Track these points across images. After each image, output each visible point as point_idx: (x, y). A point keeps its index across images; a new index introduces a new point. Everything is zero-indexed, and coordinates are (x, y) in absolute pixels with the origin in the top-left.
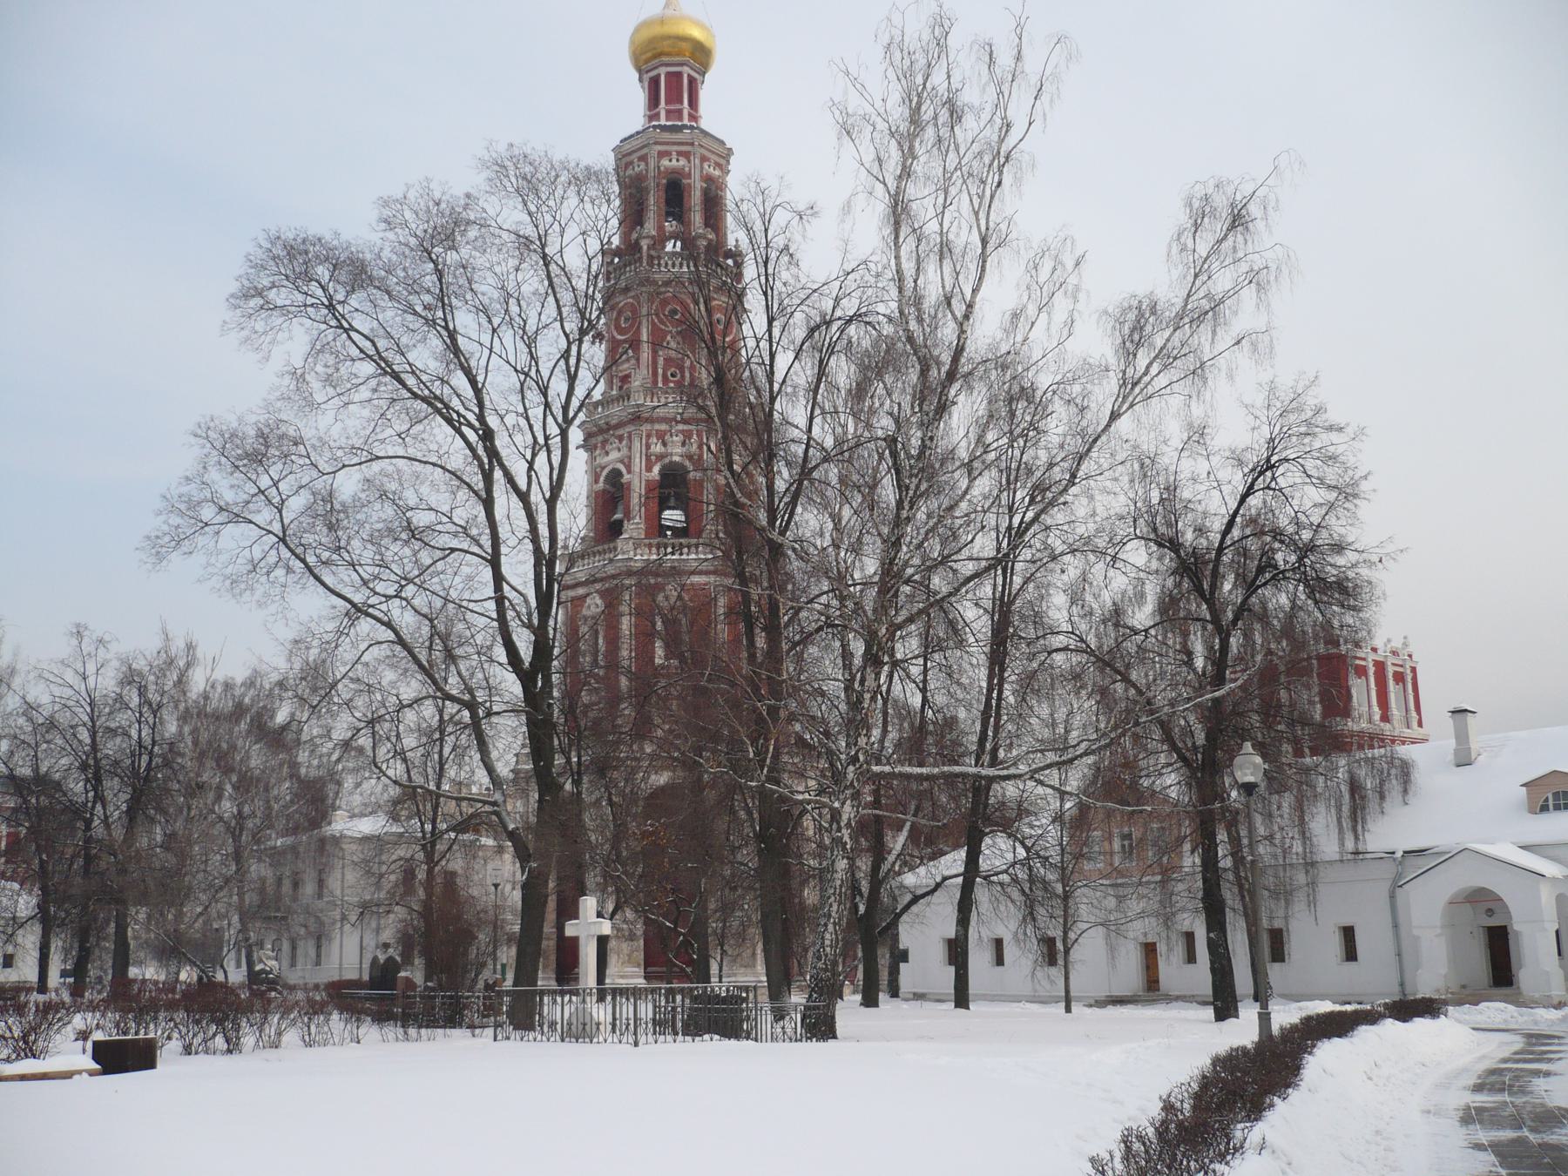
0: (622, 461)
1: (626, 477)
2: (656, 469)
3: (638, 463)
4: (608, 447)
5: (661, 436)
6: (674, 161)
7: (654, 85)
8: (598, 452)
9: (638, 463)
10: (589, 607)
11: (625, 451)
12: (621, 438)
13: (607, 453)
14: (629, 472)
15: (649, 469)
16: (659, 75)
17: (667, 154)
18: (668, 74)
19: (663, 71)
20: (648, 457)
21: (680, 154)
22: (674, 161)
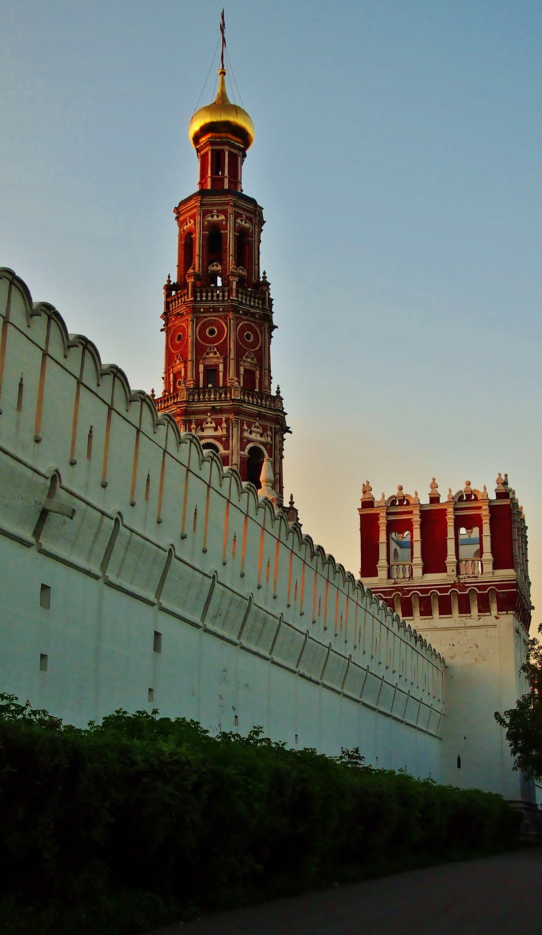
2: (246, 451)
3: (234, 442)
4: (204, 426)
5: (249, 425)
7: (218, 156)
8: (193, 426)
9: (234, 442)
11: (225, 432)
12: (219, 423)
13: (203, 430)
14: (226, 448)
15: (242, 449)
16: (223, 151)
17: (240, 215)
18: (229, 152)
19: (226, 148)
20: (242, 438)
21: (247, 218)
22: (243, 223)
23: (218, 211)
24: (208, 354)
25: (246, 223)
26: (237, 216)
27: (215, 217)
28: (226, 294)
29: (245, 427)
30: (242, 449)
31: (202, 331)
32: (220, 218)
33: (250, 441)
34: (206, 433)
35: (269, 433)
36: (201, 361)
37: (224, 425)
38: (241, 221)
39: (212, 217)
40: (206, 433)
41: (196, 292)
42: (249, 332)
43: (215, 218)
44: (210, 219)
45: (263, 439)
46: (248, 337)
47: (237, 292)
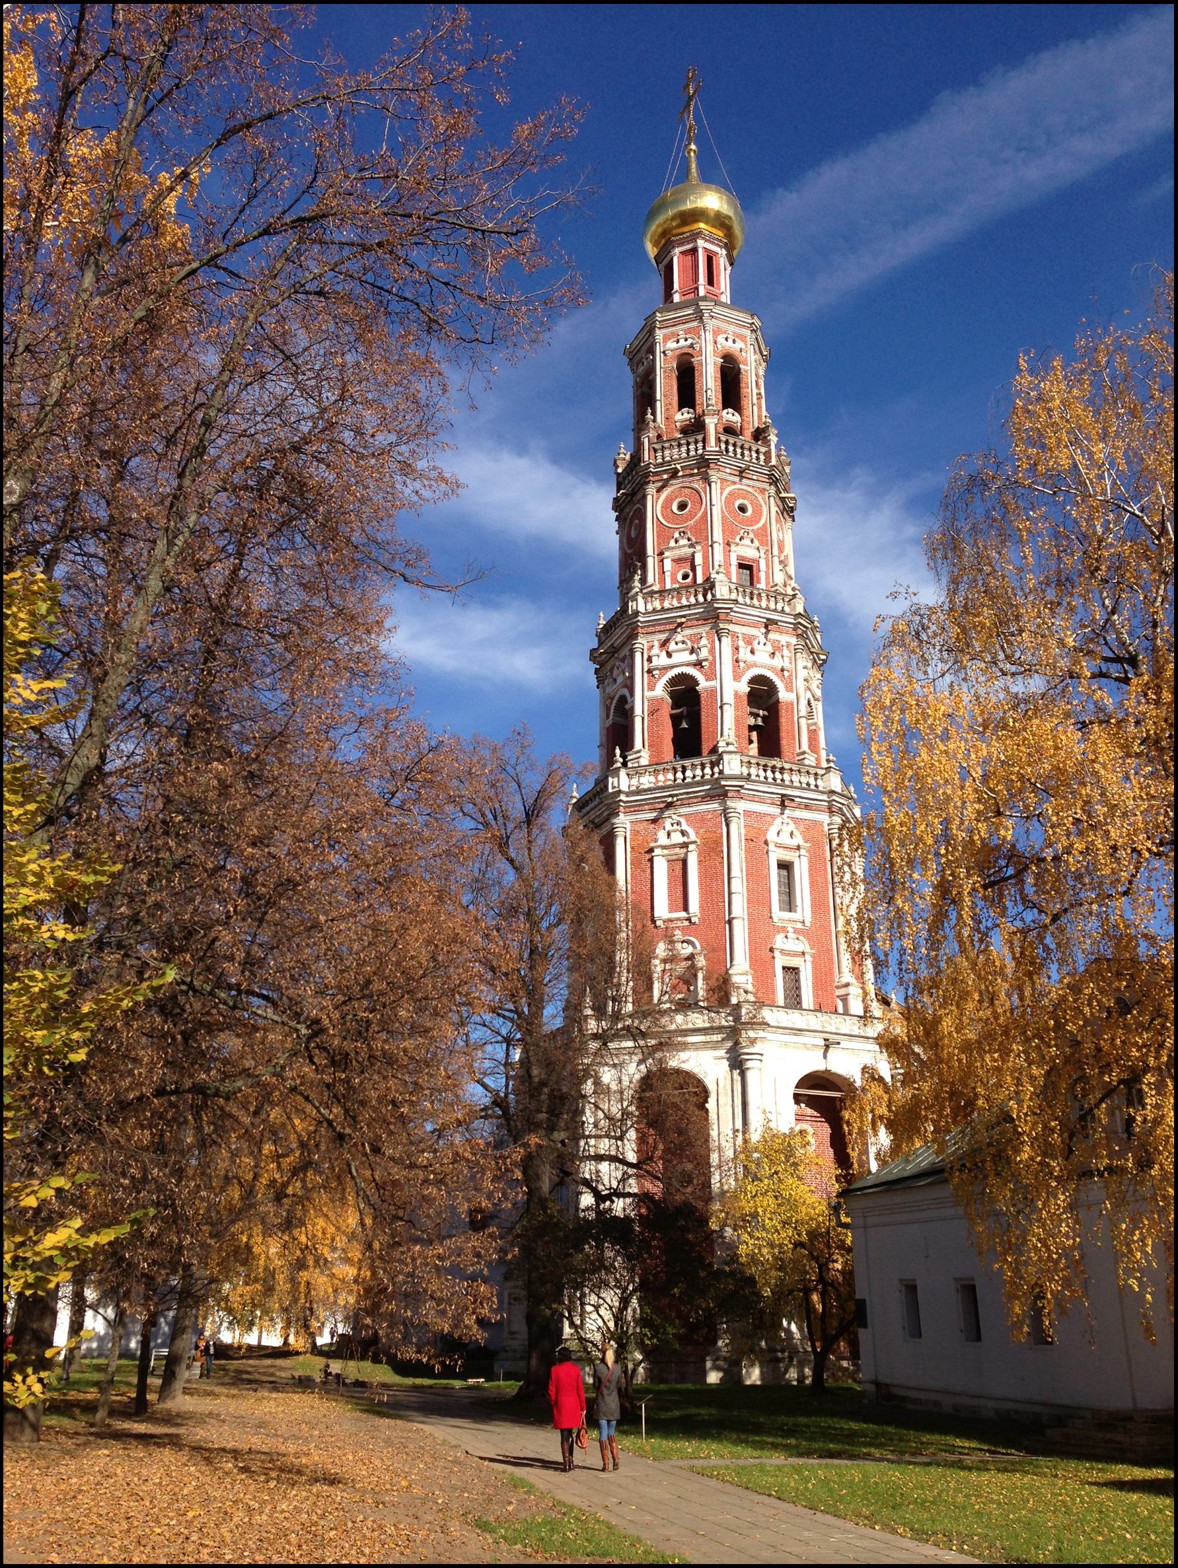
0: (698, 664)
1: (703, 684)
4: (672, 646)
5: (749, 641)
6: (730, 341)
8: (655, 651)
10: (669, 835)
22: (730, 341)
23: (687, 331)
24: (676, 541)
25: (734, 341)
26: (717, 332)
27: (682, 342)
28: (700, 445)
29: (741, 643)
30: (737, 677)
31: (667, 505)
32: (690, 341)
33: (749, 666)
34: (677, 658)
35: (786, 652)
36: (667, 554)
37: (704, 642)
38: (726, 339)
39: (678, 342)
40: (677, 658)
41: (655, 451)
42: (745, 502)
43: (682, 342)
44: (671, 345)
45: (777, 662)
46: (742, 509)
47: (718, 440)
